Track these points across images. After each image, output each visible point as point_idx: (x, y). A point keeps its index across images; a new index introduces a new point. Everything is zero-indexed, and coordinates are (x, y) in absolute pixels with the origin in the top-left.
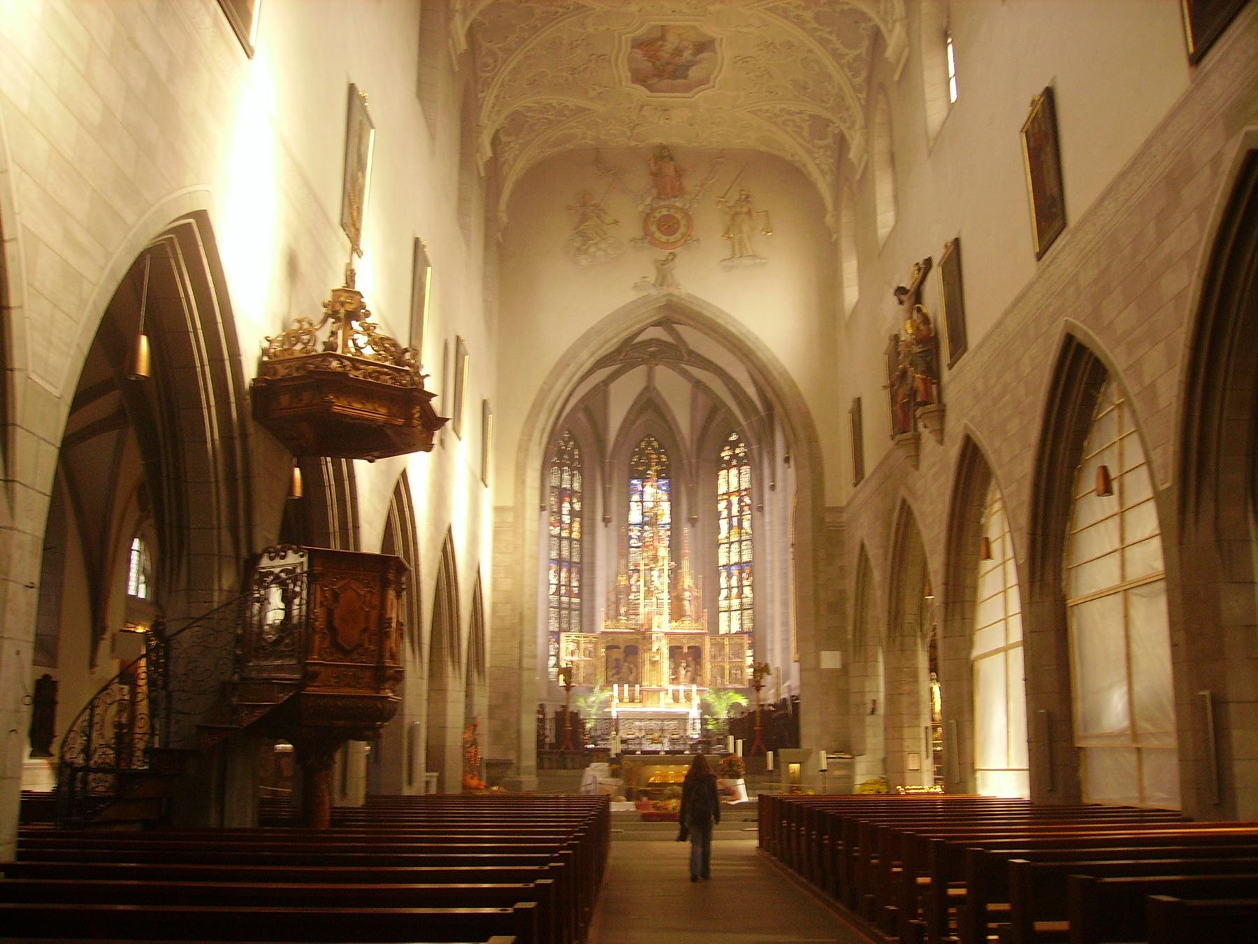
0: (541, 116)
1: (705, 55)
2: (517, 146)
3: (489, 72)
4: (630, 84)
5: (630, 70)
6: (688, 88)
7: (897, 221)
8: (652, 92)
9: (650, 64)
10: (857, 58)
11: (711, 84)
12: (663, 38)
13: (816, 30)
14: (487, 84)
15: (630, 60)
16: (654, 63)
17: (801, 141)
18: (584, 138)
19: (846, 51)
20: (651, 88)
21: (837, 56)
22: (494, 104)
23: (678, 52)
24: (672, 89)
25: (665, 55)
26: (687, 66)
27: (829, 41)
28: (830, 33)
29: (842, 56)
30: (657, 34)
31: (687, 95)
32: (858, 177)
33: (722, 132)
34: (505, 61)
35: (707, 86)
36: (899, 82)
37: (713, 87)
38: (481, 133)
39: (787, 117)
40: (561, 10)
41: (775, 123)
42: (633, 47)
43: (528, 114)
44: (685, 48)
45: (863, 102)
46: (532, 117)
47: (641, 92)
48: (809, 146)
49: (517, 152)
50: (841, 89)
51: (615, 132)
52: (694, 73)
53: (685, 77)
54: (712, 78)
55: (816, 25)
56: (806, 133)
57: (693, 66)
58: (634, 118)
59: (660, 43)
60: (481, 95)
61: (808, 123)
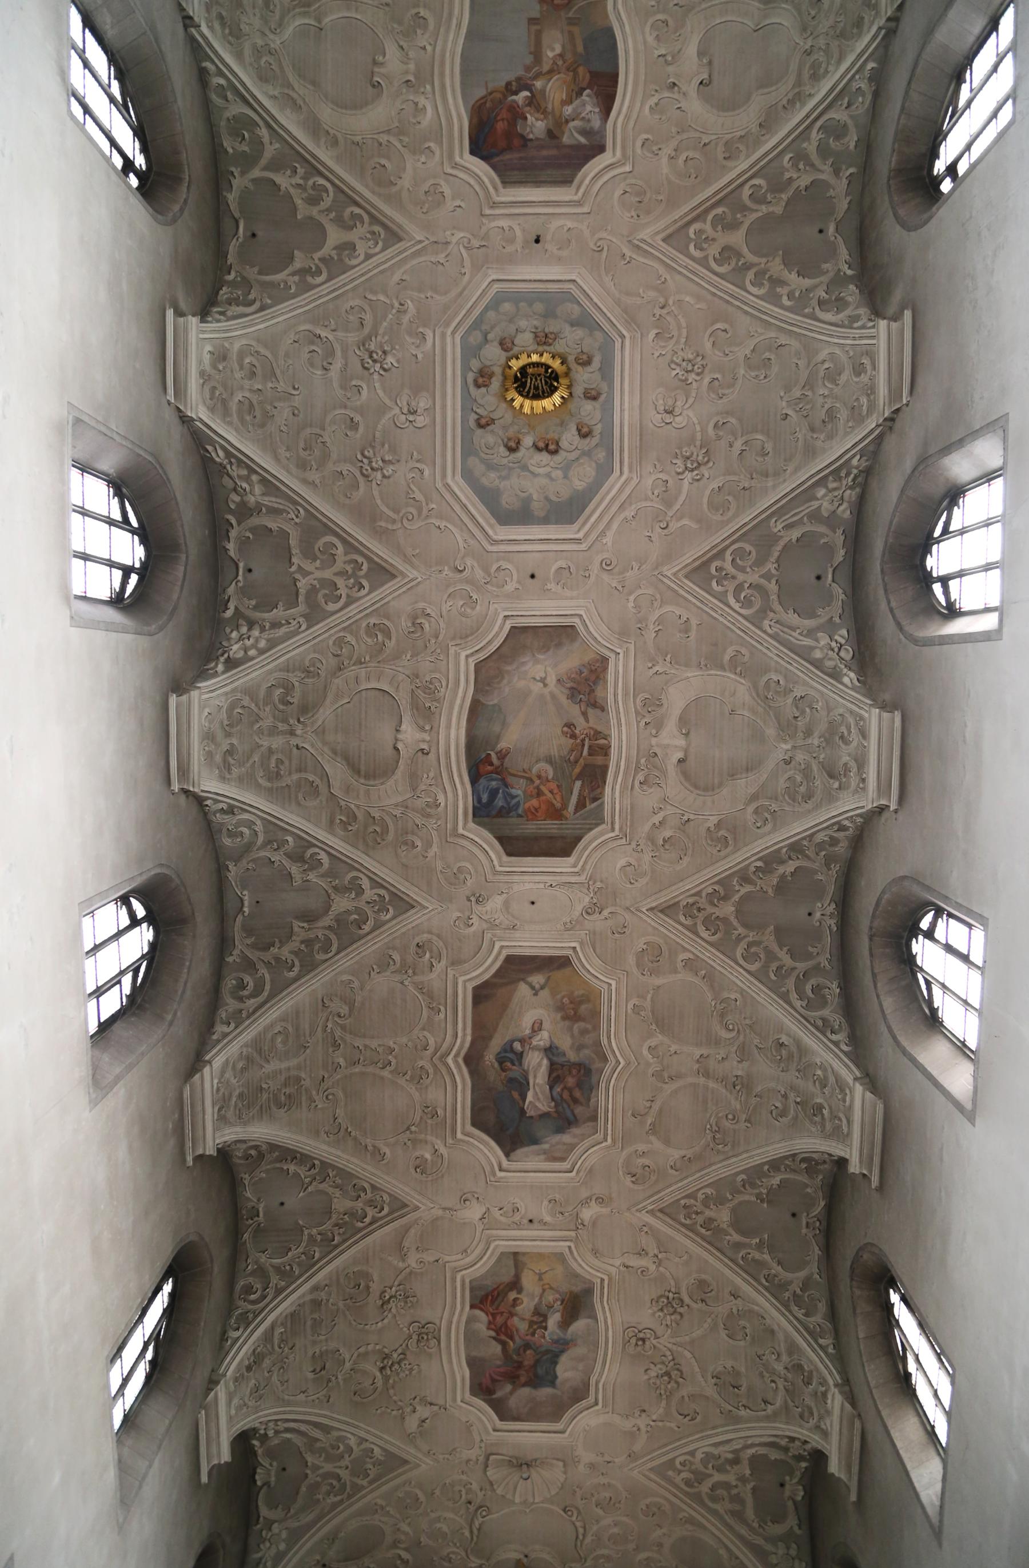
0: (328, 1467)
1: (579, 1325)
2: (284, 1535)
3: (253, 1302)
4: (468, 1394)
5: (472, 1362)
6: (556, 1411)
7: (945, 1468)
8: (502, 1418)
9: (498, 1348)
10: (806, 1285)
11: (591, 1399)
12: (515, 1284)
13: (738, 1246)
14: (245, 1321)
15: (470, 1337)
16: (504, 1344)
17: (743, 1531)
18: (395, 1544)
19: (789, 1276)
20: (502, 1411)
21: (776, 1288)
22: (249, 1368)
23: (540, 1317)
24: (533, 1414)
25: (521, 1326)
26: (554, 1357)
27: (760, 1264)
28: (760, 1247)
29: (784, 1286)
30: (506, 1275)
31: (559, 1426)
32: (853, 1497)
33: (616, 1530)
34: (279, 1291)
35: (584, 1403)
36: (881, 1188)
37: (596, 1404)
38: (217, 1383)
39: (718, 1477)
40: (371, 1212)
41: (697, 1498)
42: (472, 1307)
43: (310, 1459)
44: (550, 1307)
45: (831, 1350)
46: (316, 1468)
47: (481, 1413)
48: (759, 1541)
49: (282, 1546)
50: (793, 1349)
51: (445, 1528)
52: (566, 1370)
53: (551, 1380)
54: (593, 1381)
55: (736, 1237)
56: (750, 1513)
57: (562, 1351)
58: (475, 1486)
59: (513, 1295)
60: (235, 1334)
61: (749, 1486)
